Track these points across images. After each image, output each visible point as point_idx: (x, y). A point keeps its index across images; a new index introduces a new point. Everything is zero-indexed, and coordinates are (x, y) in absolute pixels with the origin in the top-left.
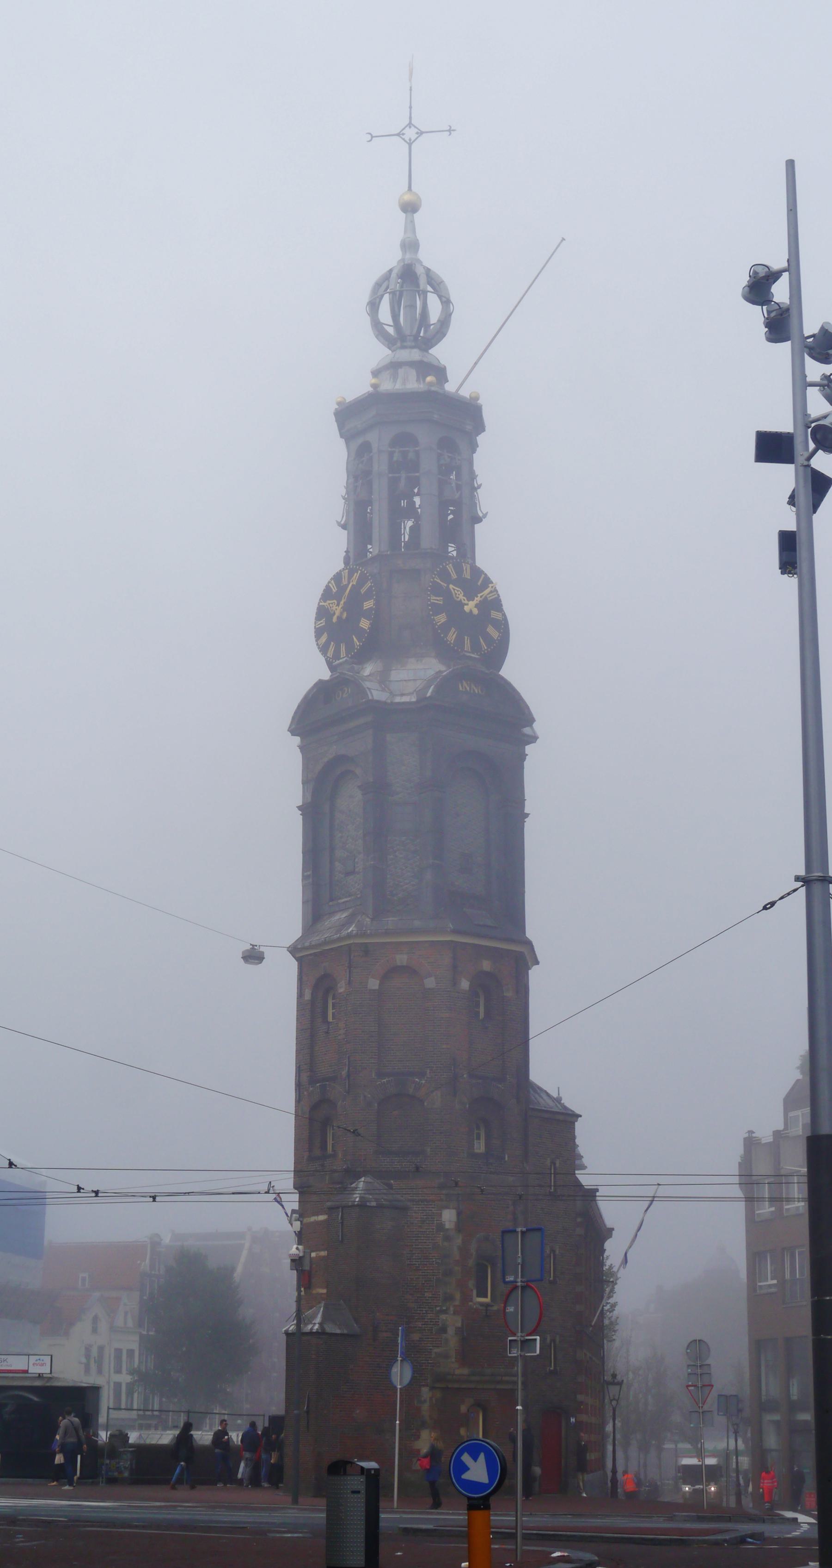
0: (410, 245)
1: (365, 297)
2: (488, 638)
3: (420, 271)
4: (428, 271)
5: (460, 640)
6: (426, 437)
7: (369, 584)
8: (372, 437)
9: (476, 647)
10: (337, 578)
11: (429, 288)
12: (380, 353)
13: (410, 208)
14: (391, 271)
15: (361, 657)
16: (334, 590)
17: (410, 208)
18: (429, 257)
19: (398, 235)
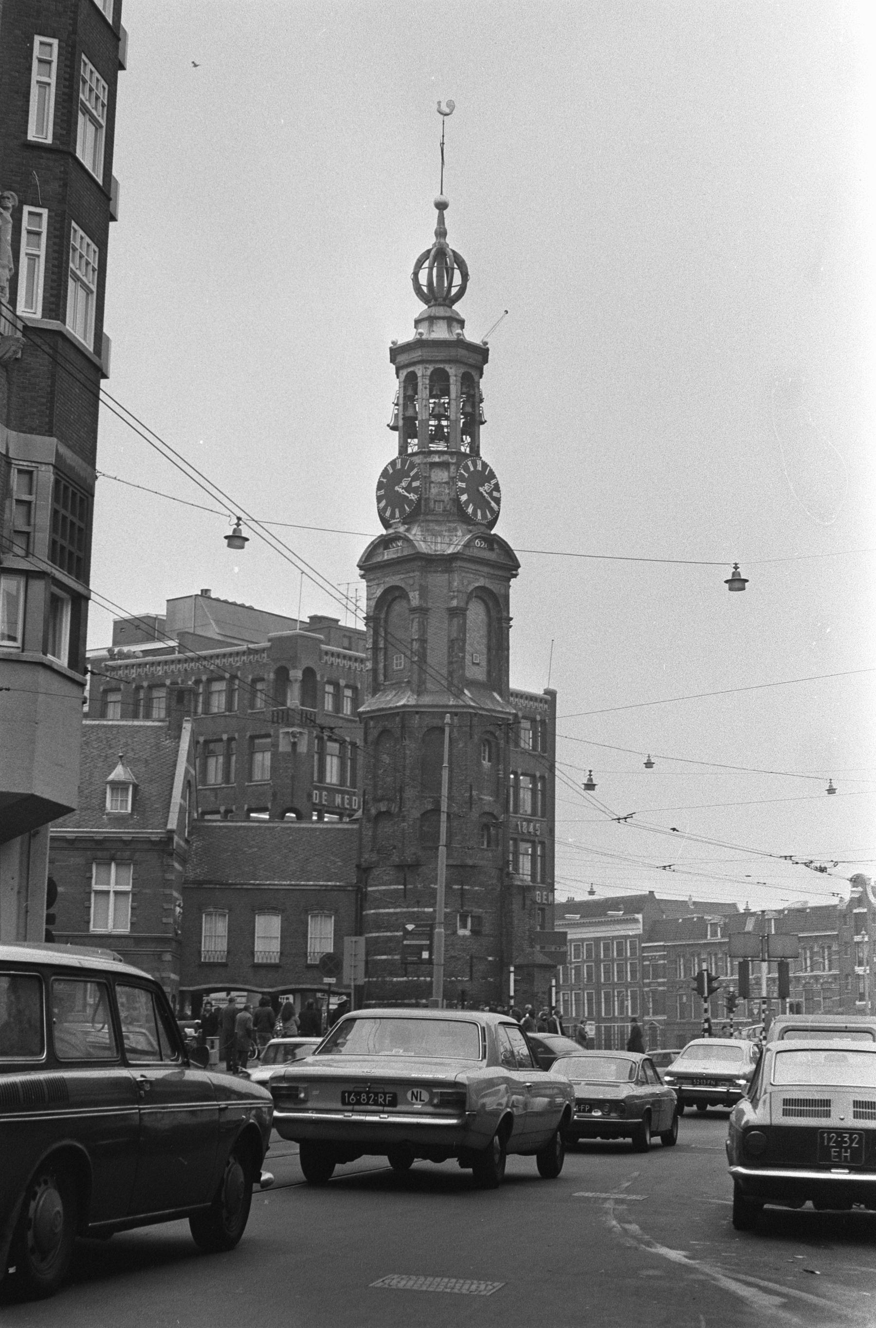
0: (441, 233)
1: (411, 270)
2: (491, 510)
4: (453, 251)
6: (452, 371)
7: (415, 470)
8: (419, 370)
9: (484, 516)
10: (393, 463)
11: (456, 266)
12: (420, 308)
13: (441, 206)
14: (429, 251)
15: (409, 520)
16: (391, 471)
17: (441, 206)
18: (453, 242)
19: (434, 225)
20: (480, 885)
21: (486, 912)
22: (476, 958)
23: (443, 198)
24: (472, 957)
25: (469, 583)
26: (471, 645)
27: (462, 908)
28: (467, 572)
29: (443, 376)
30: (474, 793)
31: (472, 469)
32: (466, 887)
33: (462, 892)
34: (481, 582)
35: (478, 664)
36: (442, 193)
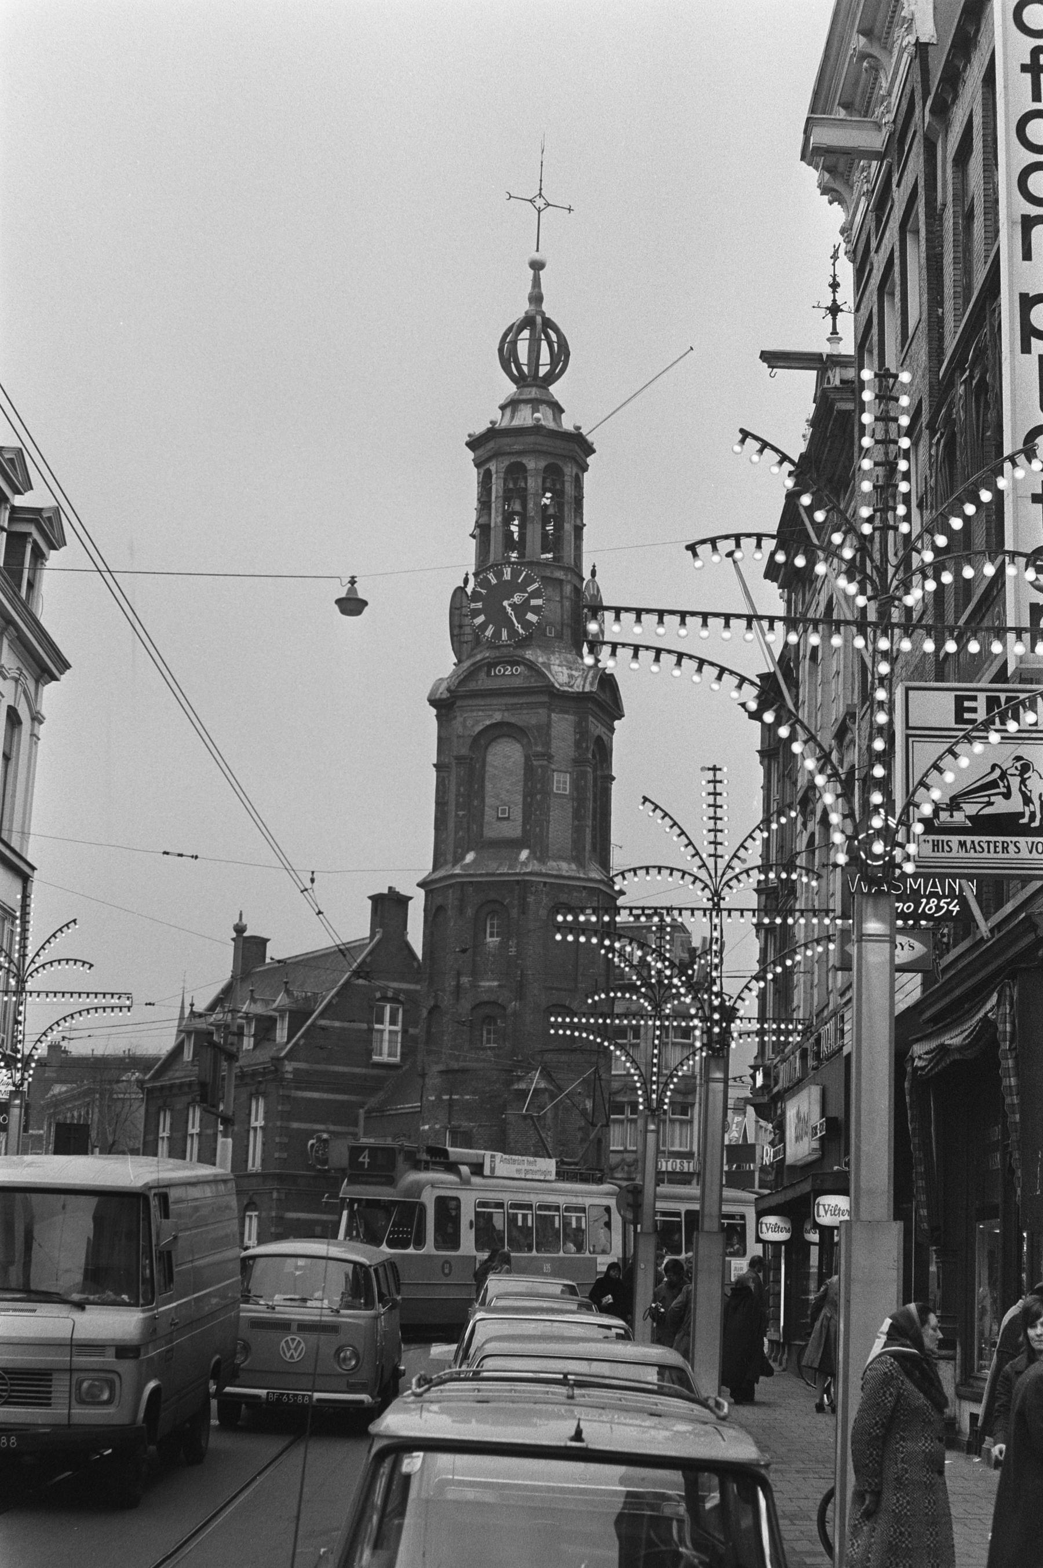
0: (536, 298)
3: (539, 319)
13: (537, 266)
17: (537, 266)
20: (473, 1093)
21: (480, 1126)
23: (537, 256)
25: (477, 722)
26: (497, 796)
27: (449, 1123)
28: (472, 711)
31: (494, 581)
32: (455, 1097)
33: (451, 1103)
34: (498, 717)
35: (508, 818)
36: (537, 250)
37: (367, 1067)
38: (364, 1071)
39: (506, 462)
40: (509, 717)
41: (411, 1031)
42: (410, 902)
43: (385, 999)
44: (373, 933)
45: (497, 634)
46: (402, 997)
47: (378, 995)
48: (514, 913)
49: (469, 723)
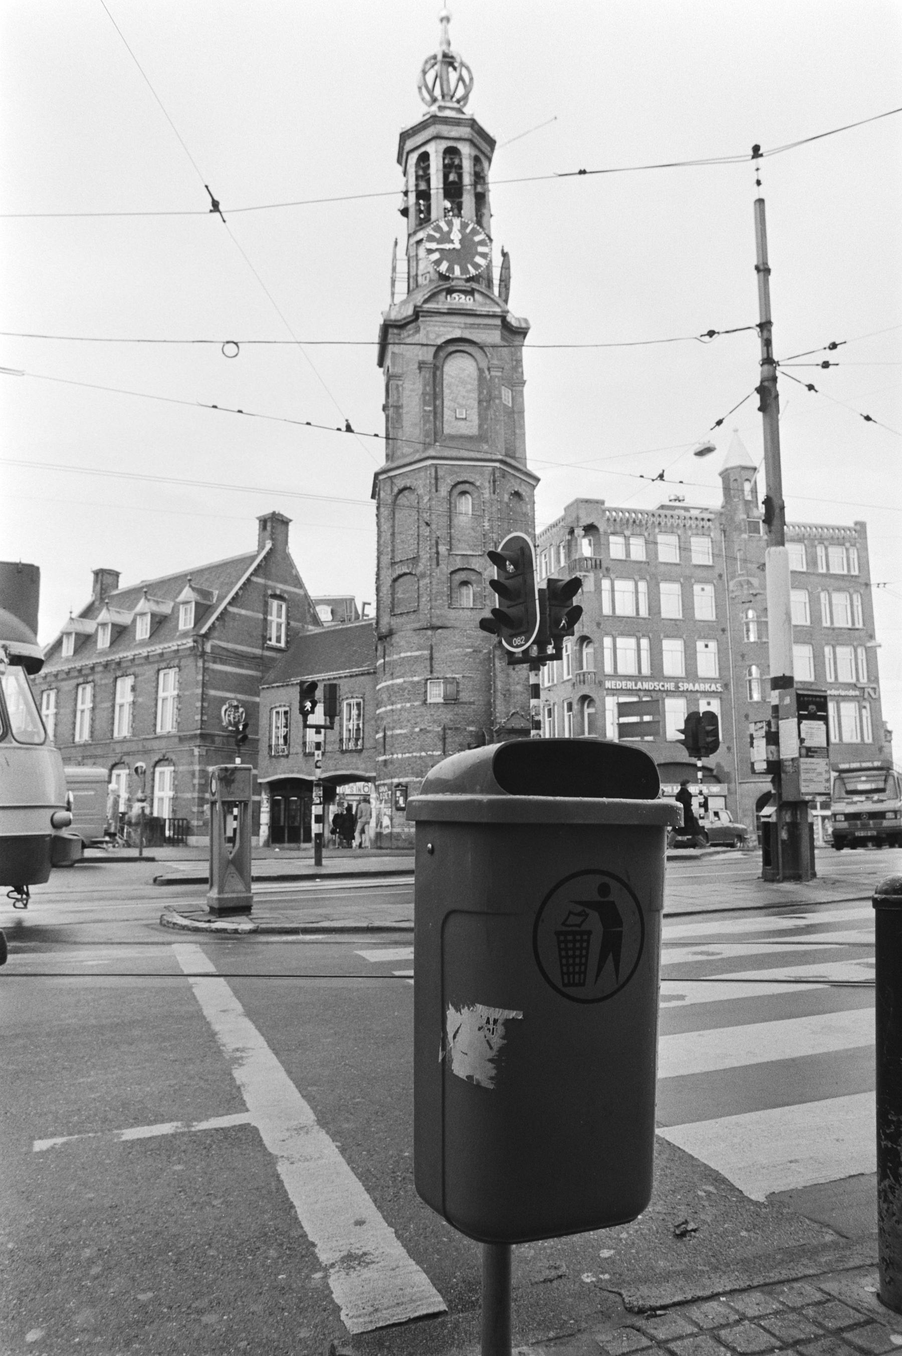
2: (477, 266)
5: (450, 269)
22: (450, 729)
24: (444, 729)
25: (438, 336)
26: (454, 400)
28: (434, 326)
29: (449, 167)
30: (443, 549)
34: (457, 334)
37: (263, 648)
38: (258, 651)
39: (444, 144)
40: (467, 335)
41: (292, 623)
42: (290, 524)
43: (275, 596)
44: (261, 546)
45: (450, 269)
46: (286, 596)
47: (270, 592)
48: (487, 494)
49: (432, 336)
